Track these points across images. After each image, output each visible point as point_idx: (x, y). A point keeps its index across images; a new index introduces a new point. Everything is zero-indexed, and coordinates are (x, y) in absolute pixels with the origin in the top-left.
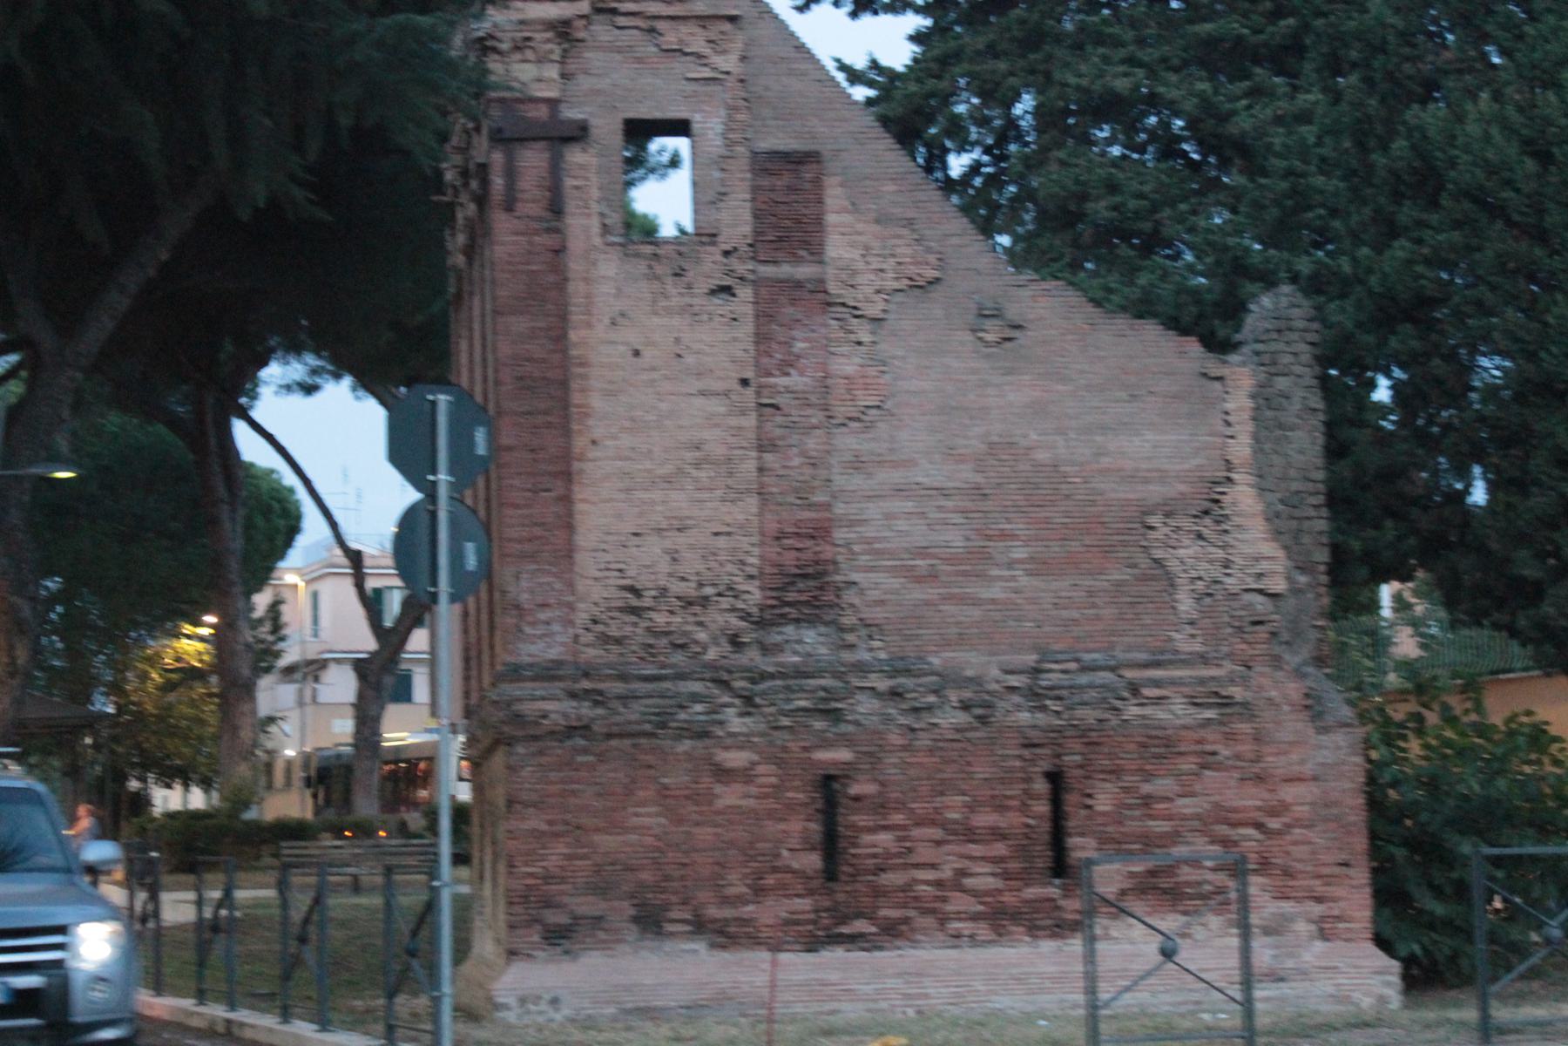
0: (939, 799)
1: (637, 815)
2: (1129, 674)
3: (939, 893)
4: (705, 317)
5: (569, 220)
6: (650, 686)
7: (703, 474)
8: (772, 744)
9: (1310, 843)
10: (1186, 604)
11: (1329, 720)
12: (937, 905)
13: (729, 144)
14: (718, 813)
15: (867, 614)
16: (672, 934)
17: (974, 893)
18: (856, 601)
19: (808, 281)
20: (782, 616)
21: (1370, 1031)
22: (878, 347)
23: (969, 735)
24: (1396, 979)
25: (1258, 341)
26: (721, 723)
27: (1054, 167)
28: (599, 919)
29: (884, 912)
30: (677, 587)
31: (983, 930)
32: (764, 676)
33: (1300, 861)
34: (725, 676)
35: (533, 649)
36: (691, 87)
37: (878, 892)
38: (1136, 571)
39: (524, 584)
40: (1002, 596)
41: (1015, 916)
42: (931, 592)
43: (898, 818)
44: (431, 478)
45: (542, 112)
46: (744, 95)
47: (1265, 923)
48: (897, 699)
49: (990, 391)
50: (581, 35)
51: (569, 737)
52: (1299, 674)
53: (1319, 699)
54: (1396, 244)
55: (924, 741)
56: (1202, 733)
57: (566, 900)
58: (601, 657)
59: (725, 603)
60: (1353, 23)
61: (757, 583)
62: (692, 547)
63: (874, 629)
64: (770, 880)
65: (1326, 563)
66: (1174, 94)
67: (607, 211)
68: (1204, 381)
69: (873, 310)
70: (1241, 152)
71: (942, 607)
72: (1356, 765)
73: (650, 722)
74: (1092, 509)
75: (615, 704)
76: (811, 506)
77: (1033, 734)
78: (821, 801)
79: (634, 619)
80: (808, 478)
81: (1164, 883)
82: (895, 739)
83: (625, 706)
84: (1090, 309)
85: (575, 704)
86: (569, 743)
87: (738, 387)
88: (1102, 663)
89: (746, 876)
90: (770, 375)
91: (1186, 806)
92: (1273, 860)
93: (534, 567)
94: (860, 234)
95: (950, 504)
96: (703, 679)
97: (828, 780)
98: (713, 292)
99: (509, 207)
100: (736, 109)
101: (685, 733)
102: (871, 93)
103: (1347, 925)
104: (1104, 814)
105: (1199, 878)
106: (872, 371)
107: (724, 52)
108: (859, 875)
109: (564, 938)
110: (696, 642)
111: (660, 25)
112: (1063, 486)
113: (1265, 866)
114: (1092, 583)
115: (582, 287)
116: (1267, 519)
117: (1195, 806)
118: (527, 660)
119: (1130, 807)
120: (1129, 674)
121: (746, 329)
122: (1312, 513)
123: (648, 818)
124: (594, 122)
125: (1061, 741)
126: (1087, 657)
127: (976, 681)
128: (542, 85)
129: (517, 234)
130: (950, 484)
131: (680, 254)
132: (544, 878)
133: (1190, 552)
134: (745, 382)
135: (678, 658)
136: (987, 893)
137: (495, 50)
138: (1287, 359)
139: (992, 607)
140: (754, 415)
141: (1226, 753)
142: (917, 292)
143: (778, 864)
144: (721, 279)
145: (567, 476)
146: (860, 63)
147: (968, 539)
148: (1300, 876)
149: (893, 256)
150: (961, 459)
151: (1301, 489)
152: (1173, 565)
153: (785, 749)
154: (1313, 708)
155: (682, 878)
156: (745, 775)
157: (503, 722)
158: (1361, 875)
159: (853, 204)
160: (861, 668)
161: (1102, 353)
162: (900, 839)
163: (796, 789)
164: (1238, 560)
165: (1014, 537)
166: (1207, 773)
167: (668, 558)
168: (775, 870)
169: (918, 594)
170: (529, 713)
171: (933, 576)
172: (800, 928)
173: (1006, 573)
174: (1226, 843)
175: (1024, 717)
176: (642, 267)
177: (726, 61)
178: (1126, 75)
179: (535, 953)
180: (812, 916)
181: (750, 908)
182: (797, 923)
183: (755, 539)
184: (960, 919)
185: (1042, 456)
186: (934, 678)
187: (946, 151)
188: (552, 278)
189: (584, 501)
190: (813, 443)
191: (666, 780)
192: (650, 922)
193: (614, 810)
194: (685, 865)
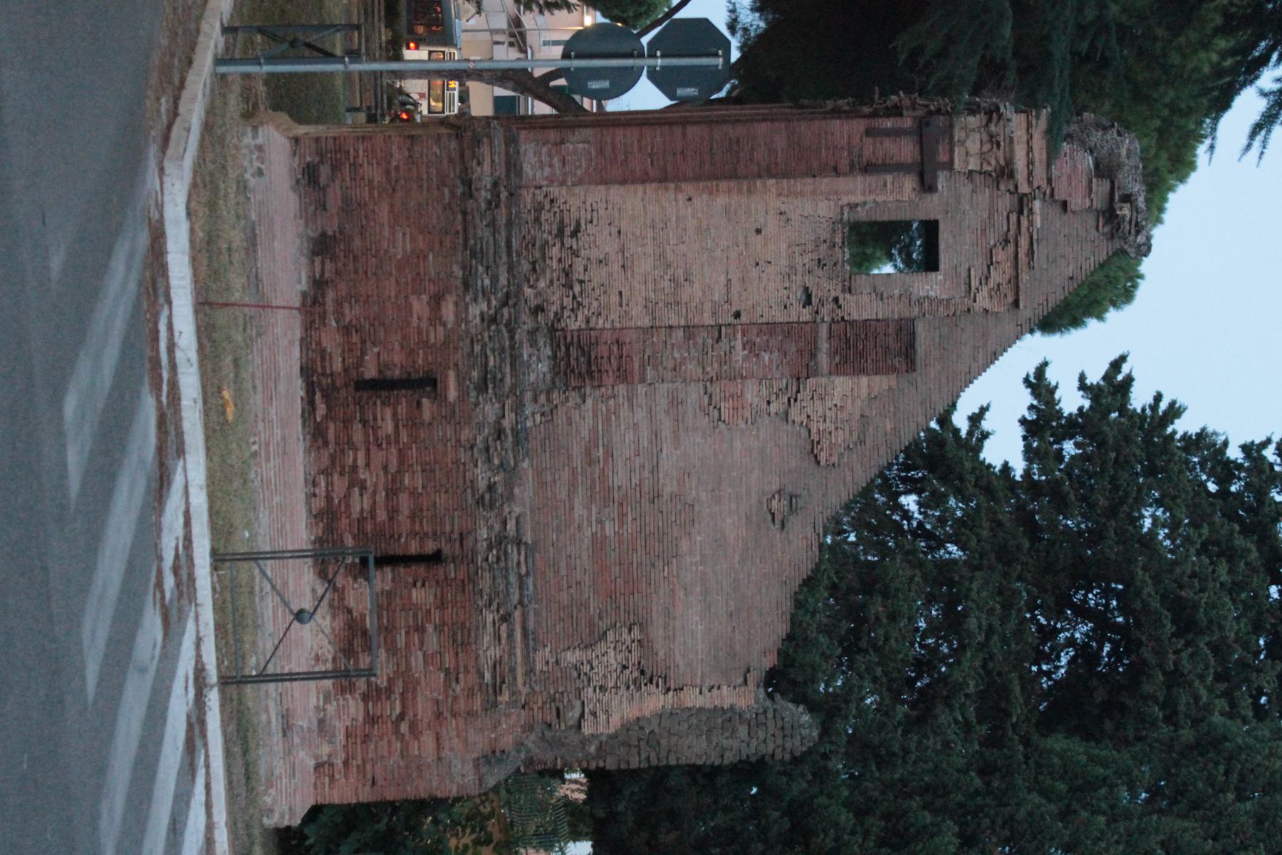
0: (419, 468)
1: (404, 234)
2: (517, 614)
4: (787, 285)
5: (860, 178)
6: (503, 244)
7: (667, 283)
8: (460, 338)
9: (389, 757)
10: (571, 657)
11: (483, 770)
13: (920, 301)
14: (406, 297)
15: (561, 411)
16: (313, 262)
17: (347, 496)
18: (570, 404)
19: (816, 364)
20: (558, 346)
21: (243, 781)
22: (766, 417)
23: (469, 491)
24: (286, 823)
25: (775, 711)
26: (475, 300)
27: (908, 573)
28: (325, 209)
29: (331, 425)
30: (579, 264)
31: (319, 503)
32: (512, 332)
33: (376, 748)
34: (511, 303)
35: (531, 154)
36: (964, 274)
37: (347, 423)
38: (596, 620)
39: (581, 146)
40: (576, 515)
41: (330, 529)
42: (578, 462)
43: (404, 437)
44: (659, 53)
45: (943, 157)
46: (958, 313)
47: (328, 722)
48: (496, 436)
49: (733, 506)
50: (1002, 187)
51: (463, 182)
52: (519, 745)
53: (500, 761)
54: (851, 815)
55: (463, 456)
56: (473, 671)
57: (338, 182)
58: (525, 206)
59: (568, 302)
60: (1020, 782)
61: (583, 326)
62: (610, 275)
63: (550, 418)
64: (355, 338)
66: (966, 665)
67: (867, 207)
68: (742, 671)
69: (794, 413)
70: (922, 717)
71: (566, 468)
72: (450, 792)
73: (476, 244)
75: (489, 218)
76: (643, 367)
77: (471, 538)
78: (417, 377)
79: (555, 232)
80: (665, 363)
81: (358, 642)
82: (466, 434)
83: (487, 226)
84: (798, 582)
85: (489, 186)
86: (458, 182)
87: (734, 310)
88: (526, 593)
89: (358, 319)
90: (744, 335)
91: (417, 660)
93: (594, 154)
94: (853, 401)
95: (646, 474)
96: (509, 285)
97: (433, 383)
98: (806, 289)
99: (868, 132)
100: (947, 307)
101: (467, 273)
102: (963, 433)
103: (327, 786)
104: (410, 597)
106: (747, 414)
107: (991, 297)
108: (360, 408)
109: (309, 178)
110: (538, 280)
111: (1011, 248)
112: (661, 564)
113: (371, 720)
114: (587, 583)
115: (809, 188)
116: (638, 719)
117: (416, 667)
118: (522, 151)
119: (415, 615)
120: (517, 614)
121: (779, 316)
122: (643, 757)
123: (402, 245)
124: (935, 197)
125: (465, 562)
126: (530, 582)
127: (510, 497)
128: (963, 155)
130: (661, 476)
131: (835, 264)
132: (354, 164)
133: (612, 661)
134: (737, 315)
135: (526, 266)
136: (348, 506)
137: (990, 120)
138: (761, 735)
139: (567, 506)
140: (712, 322)
141: (458, 689)
142: (809, 447)
143: (368, 344)
144: (817, 295)
145: (663, 179)
146: (986, 425)
147: (619, 487)
149: (836, 428)
150: (681, 483)
152: (602, 647)
153: (456, 348)
154: (493, 756)
155: (356, 272)
156: (436, 319)
157: (474, 130)
158: (366, 795)
159: (876, 397)
160: (519, 407)
161: (764, 591)
162: (388, 437)
163: (425, 359)
165: (622, 524)
166: (442, 676)
167: (602, 257)
168: (363, 342)
169: (577, 451)
170: (482, 150)
171: (591, 462)
172: (319, 363)
173: (594, 518)
174: (389, 690)
175: (484, 533)
176: (825, 235)
177: (984, 298)
178: (980, 627)
179: (297, 158)
180: (328, 372)
181: (334, 324)
182: (323, 359)
183: (618, 325)
184: (327, 487)
185: (684, 545)
186: (512, 462)
187: (919, 494)
188: (815, 165)
189: (645, 193)
190: (691, 368)
192: (322, 247)
193: (408, 218)
194: (366, 272)
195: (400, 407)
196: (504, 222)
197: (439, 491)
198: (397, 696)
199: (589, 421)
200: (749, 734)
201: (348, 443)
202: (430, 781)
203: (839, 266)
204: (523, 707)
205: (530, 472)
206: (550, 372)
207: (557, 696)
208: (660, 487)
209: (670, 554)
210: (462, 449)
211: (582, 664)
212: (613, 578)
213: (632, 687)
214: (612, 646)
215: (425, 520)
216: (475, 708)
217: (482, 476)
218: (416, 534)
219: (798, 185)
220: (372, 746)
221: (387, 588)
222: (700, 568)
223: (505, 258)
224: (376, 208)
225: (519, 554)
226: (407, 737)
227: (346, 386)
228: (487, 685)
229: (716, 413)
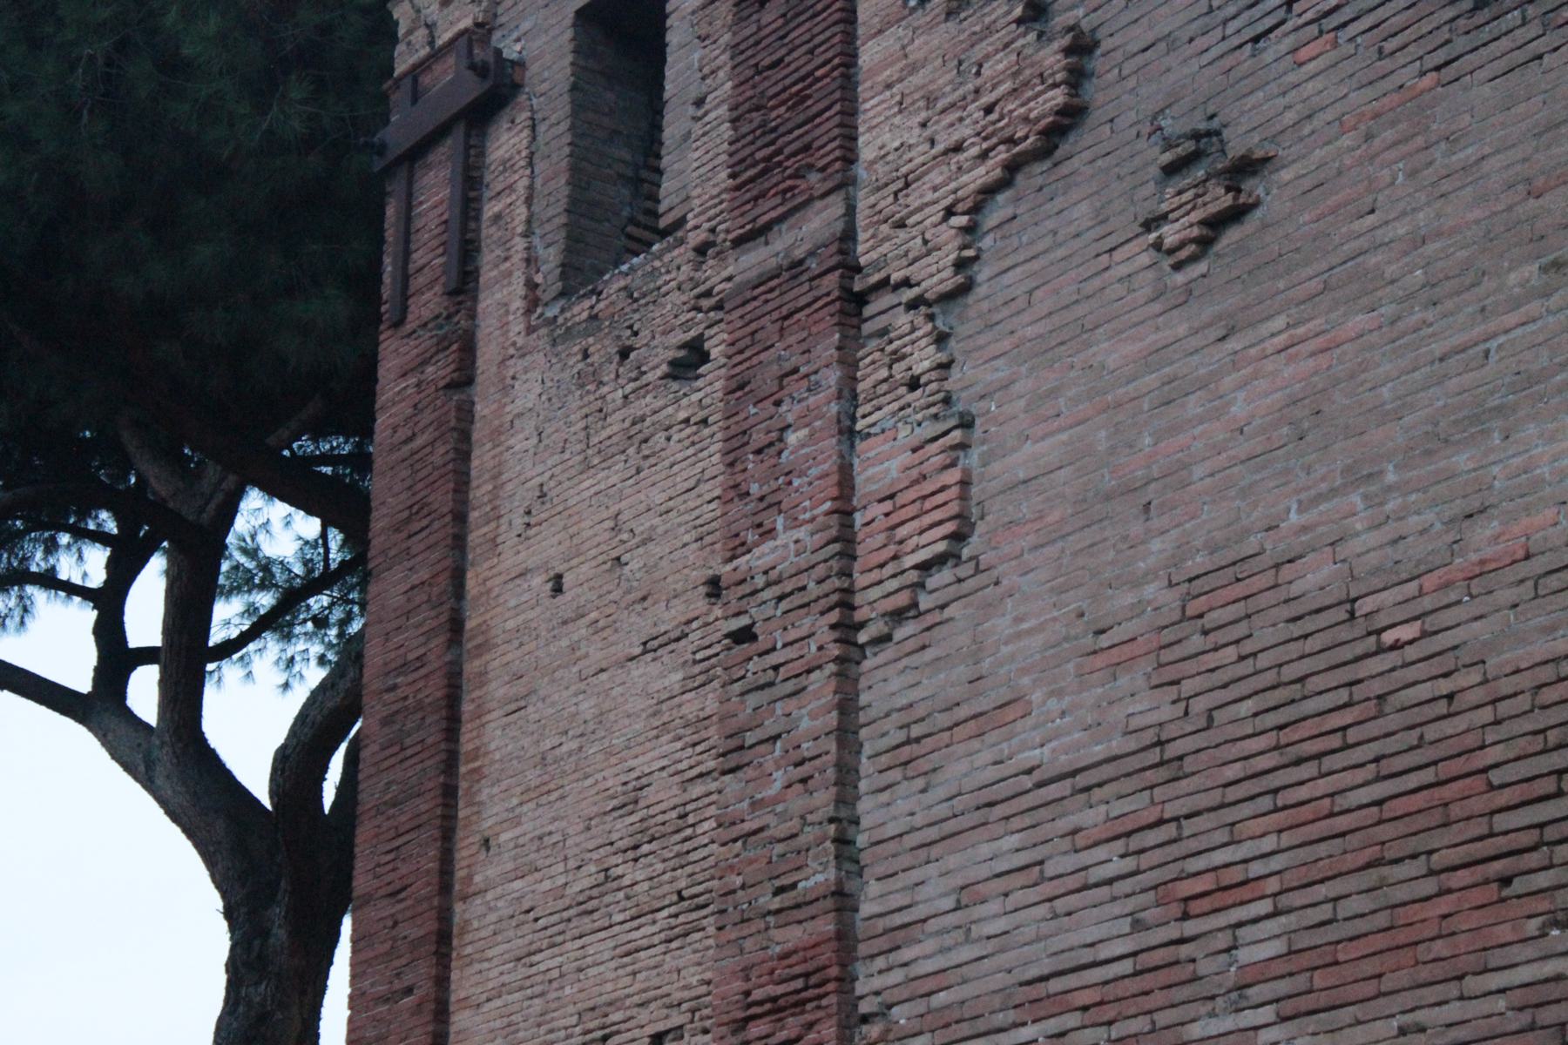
4: (662, 435)
5: (488, 301)
22: (955, 373)
45: (445, 73)
49: (1194, 406)
74: (1448, 727)
87: (701, 605)
94: (913, 69)
95: (1091, 818)
114: (1453, 1011)
129: (404, 375)
130: (1099, 751)
147: (1138, 926)
203: (636, 281)
208: (1132, 744)
209: (1344, 633)
212: (1429, 886)
219: (480, 491)
222: (1391, 477)
229: (932, 583)
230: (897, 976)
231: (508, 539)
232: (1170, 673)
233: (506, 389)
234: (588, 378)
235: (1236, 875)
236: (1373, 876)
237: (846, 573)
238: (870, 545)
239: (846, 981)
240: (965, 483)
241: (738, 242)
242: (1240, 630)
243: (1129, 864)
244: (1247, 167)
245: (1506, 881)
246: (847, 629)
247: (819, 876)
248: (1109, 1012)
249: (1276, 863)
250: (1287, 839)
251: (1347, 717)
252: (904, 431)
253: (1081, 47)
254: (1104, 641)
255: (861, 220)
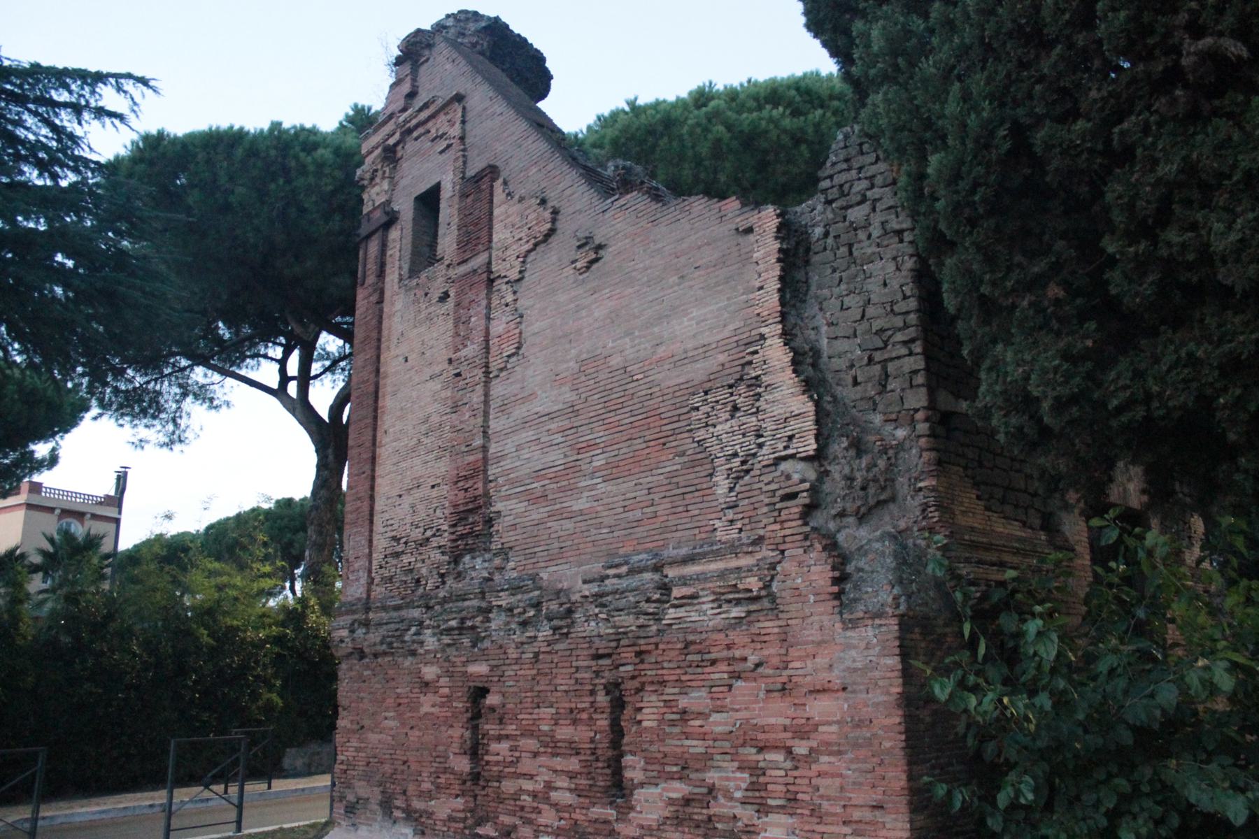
0: (536, 711)
1: (386, 718)
2: (672, 572)
3: (535, 805)
5: (387, 279)
6: (394, 614)
9: (841, 775)
12: (533, 816)
22: (519, 302)
23: (557, 647)
38: (685, 459)
40: (588, 505)
42: (539, 513)
45: (378, 214)
49: (584, 313)
56: (733, 635)
65: (924, 408)
68: (741, 239)
71: (549, 525)
74: (651, 402)
79: (394, 562)
81: (699, 814)
85: (364, 631)
92: (800, 796)
94: (508, 217)
95: (553, 426)
105: (730, 812)
111: (430, 124)
114: (649, 479)
117: (726, 724)
122: (904, 351)
127: (567, 592)
130: (556, 408)
133: (727, 426)
139: (580, 518)
141: (753, 659)
145: (373, 459)
147: (566, 456)
148: (830, 819)
151: (887, 326)
164: (769, 425)
166: (740, 683)
168: (445, 770)
172: (457, 825)
174: (756, 771)
180: (462, 815)
181: (433, 803)
185: (616, 361)
186: (537, 593)
191: (398, 691)
194: (405, 762)
195: (491, 732)
196: (384, 614)
197: (556, 686)
198: (760, 757)
199: (512, 504)
200: (859, 204)
201: (515, 800)
202: (877, 705)
204: (783, 552)
205: (551, 569)
206: (483, 555)
207: (767, 501)
208: (565, 406)
209: (626, 376)
210: (524, 656)
211: (731, 469)
212: (644, 445)
213: (759, 390)
214: (711, 429)
215: (579, 706)
216: (776, 630)
217: (545, 632)
218: (591, 718)
219: (385, 333)
220: (825, 804)
221: (642, 763)
223: (404, 613)
224: (370, 746)
225: (608, 577)
226: (814, 744)
227: (475, 797)
228: (749, 613)
230: (500, 469)
231: (393, 346)
232: (575, 387)
233: (393, 304)
234: (416, 301)
235: (593, 442)
236: (629, 442)
237: (487, 358)
238: (494, 350)
239: (485, 471)
240: (521, 333)
241: (459, 264)
242: (594, 376)
243: (563, 439)
244: (600, 247)
245: (664, 444)
246: (487, 373)
247: (478, 442)
248: (557, 479)
249: (603, 439)
250: (607, 433)
251: (621, 400)
252: (504, 318)
253: (555, 212)
254: (558, 378)
255: (493, 259)
